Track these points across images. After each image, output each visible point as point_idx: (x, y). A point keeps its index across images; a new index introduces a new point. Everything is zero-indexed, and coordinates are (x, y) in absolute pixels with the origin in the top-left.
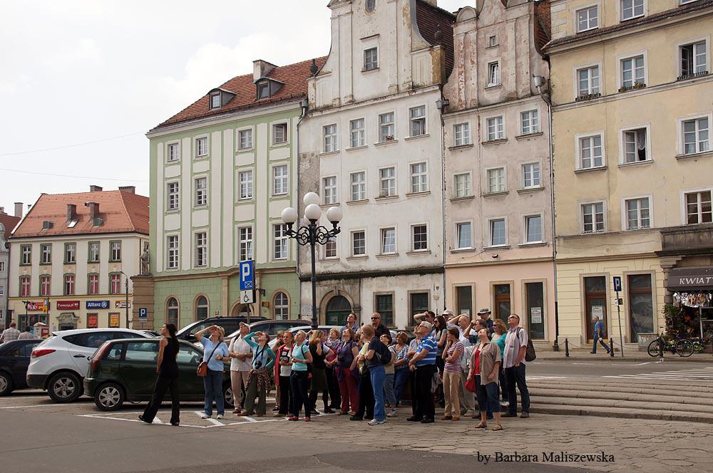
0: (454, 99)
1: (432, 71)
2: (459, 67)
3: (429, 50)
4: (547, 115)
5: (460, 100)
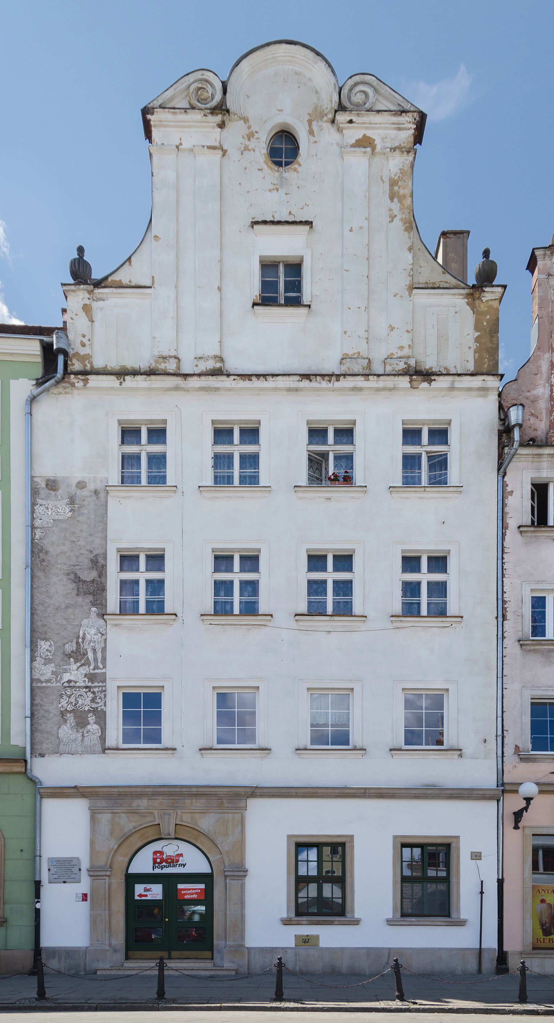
1: (474, 346)
3: (469, 295)
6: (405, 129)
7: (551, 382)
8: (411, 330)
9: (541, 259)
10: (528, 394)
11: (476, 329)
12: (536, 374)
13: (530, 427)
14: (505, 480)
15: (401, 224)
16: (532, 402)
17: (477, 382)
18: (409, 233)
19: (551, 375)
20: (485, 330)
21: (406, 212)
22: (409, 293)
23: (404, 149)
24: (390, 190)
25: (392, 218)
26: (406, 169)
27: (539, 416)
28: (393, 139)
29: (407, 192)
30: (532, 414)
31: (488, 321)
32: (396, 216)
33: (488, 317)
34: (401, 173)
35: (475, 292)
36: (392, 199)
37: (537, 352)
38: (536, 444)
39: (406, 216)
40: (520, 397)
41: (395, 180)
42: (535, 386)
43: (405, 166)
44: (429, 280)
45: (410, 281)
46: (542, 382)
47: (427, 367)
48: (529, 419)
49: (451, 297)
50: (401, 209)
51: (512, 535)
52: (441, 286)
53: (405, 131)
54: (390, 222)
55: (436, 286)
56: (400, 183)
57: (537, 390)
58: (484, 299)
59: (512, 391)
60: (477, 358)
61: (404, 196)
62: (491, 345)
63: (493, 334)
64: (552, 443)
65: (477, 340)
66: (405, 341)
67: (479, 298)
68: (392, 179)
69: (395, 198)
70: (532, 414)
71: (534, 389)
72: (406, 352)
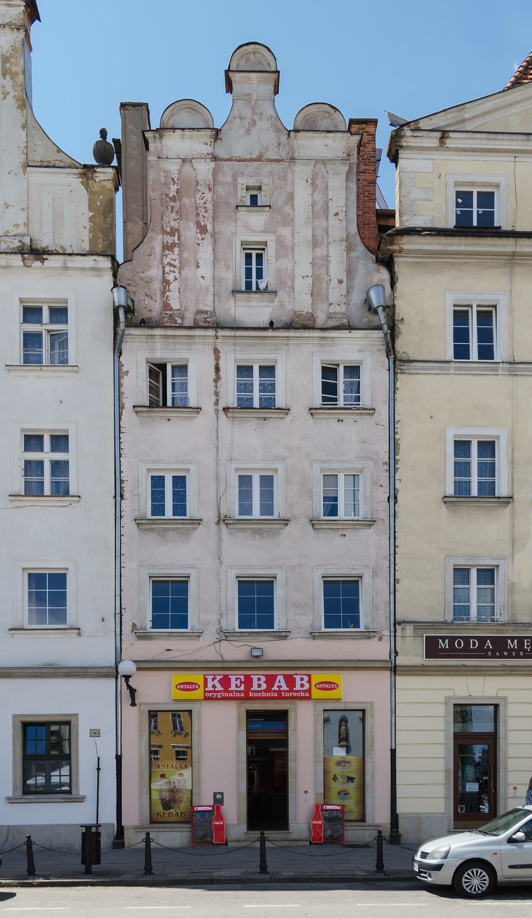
0: (147, 301)
1: (88, 225)
2: (164, 232)
4: (384, 376)
5: (166, 306)
6: (14, 6)
7: (163, 264)
8: (26, 208)
9: (152, 142)
10: (143, 275)
11: (90, 210)
12: (150, 255)
13: (145, 308)
14: (120, 360)
15: (14, 101)
16: (147, 283)
17: (89, 262)
18: (22, 110)
19: (163, 256)
20: (99, 210)
21: (19, 89)
22: (23, 170)
23: (13, 27)
24: (2, 67)
25: (6, 94)
26: (17, 46)
27: (153, 296)
28: (3, 15)
29: (19, 69)
30: (147, 295)
31: (101, 201)
32: (8, 93)
33: (101, 197)
34: (13, 50)
35: (88, 172)
36: (4, 76)
37: (150, 233)
38: (146, 324)
39: (18, 93)
40: (135, 278)
41: (7, 57)
42: (149, 267)
43: (17, 43)
44: (44, 159)
45: (24, 159)
46: (156, 263)
47: (44, 246)
48: (144, 300)
49: (66, 176)
50: (13, 87)
51: (128, 414)
52: (57, 165)
53: (15, 8)
54: (3, 99)
55: (51, 165)
56: (11, 60)
57: (152, 271)
58: (97, 180)
59: (128, 272)
60: (91, 237)
61: (17, 74)
62: (106, 226)
63: (106, 214)
64: (163, 324)
65: (91, 219)
66: (21, 219)
67: (92, 178)
68: (4, 55)
69: (8, 75)
70: (147, 295)
71: (148, 270)
72: (22, 230)
